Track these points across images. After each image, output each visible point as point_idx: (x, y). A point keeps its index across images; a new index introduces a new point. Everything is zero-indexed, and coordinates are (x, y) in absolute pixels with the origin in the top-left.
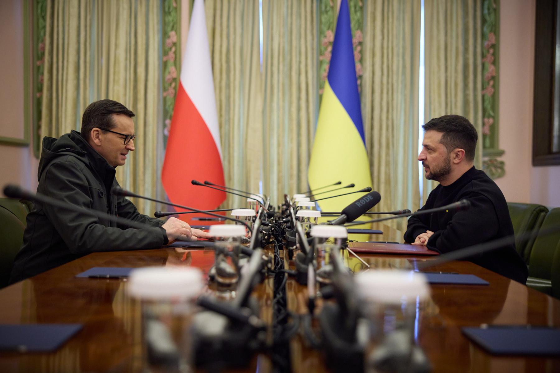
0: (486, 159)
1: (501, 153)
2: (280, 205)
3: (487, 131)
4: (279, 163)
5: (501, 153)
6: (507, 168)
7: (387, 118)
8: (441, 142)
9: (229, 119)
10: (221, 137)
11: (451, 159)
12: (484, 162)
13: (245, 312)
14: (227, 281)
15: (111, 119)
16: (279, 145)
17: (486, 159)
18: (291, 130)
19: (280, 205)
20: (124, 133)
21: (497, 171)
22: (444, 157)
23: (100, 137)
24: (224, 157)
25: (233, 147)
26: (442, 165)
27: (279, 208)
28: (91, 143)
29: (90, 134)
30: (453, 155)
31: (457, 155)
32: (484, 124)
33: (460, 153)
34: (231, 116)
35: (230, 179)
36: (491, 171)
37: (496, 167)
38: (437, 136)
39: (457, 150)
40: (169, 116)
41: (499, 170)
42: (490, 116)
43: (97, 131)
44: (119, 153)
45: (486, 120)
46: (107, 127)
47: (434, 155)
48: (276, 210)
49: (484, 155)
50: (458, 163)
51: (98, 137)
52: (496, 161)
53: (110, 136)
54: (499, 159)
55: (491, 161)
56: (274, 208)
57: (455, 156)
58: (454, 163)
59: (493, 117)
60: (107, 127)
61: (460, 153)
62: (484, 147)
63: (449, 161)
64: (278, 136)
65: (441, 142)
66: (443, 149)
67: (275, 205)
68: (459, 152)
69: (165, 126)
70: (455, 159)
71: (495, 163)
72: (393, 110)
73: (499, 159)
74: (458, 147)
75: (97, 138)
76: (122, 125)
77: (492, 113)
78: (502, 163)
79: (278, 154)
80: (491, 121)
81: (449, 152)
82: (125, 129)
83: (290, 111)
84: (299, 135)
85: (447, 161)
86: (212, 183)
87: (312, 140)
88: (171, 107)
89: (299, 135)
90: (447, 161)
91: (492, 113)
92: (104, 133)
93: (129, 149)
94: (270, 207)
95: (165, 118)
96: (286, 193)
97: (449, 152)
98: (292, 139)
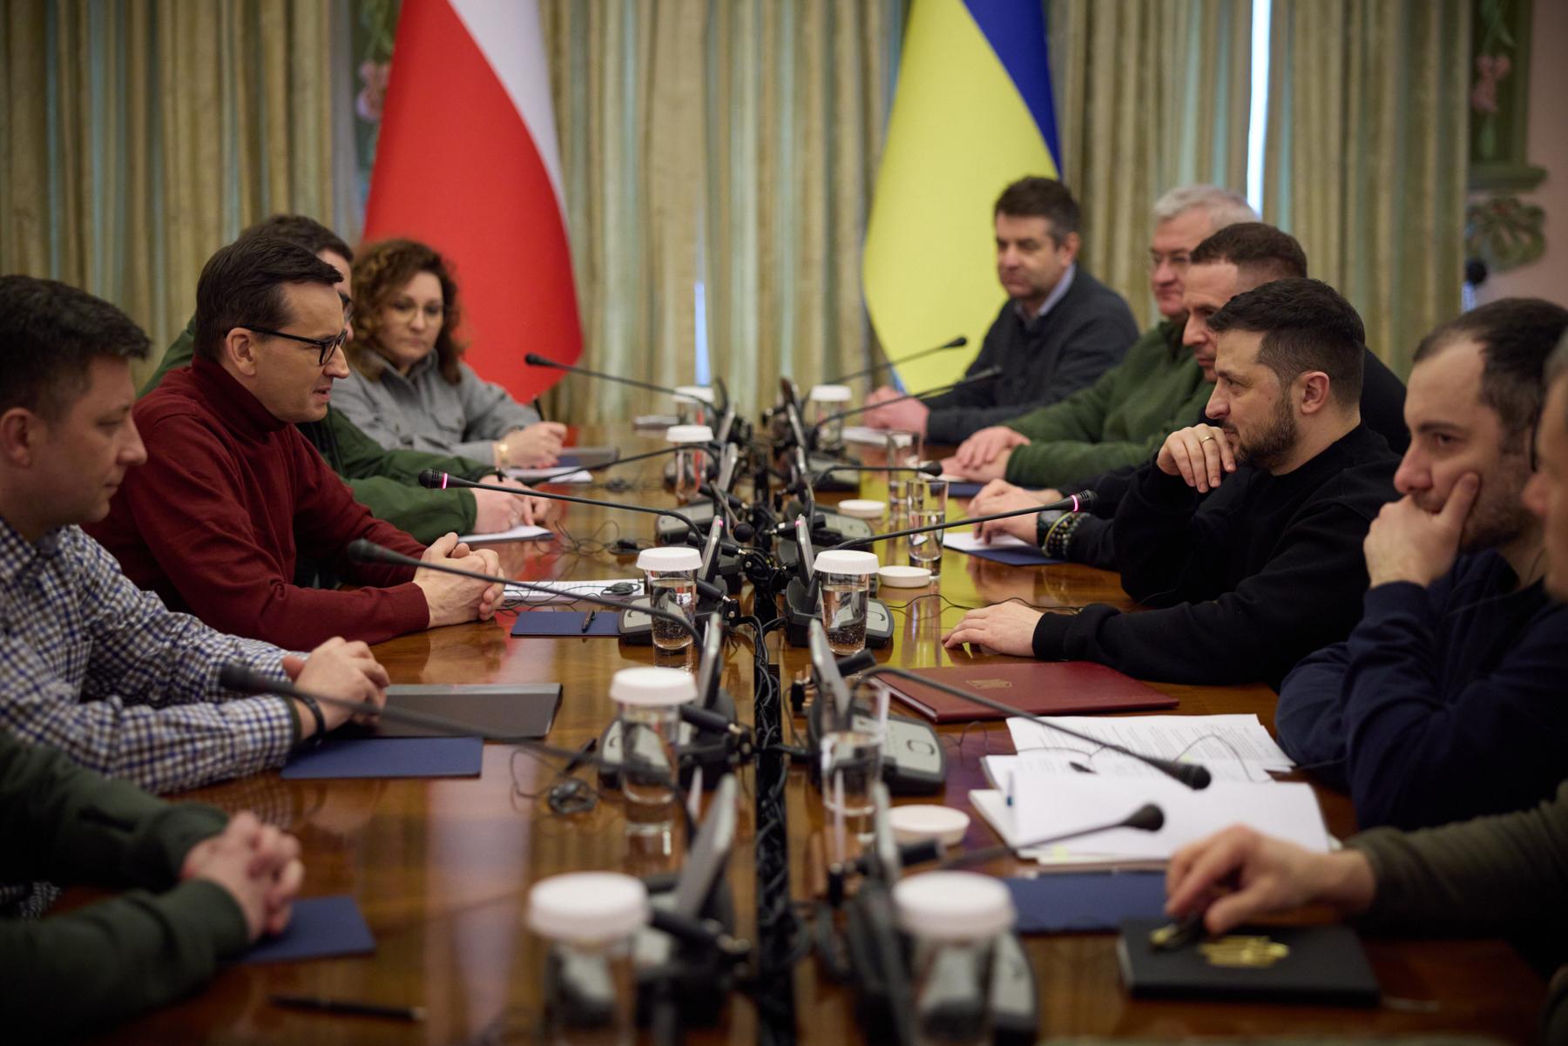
0: (1482, 198)
1: (1535, 178)
2: (769, 412)
3: (1487, 101)
4: (763, 221)
5: (1535, 178)
6: (1550, 230)
7: (1142, 59)
9: (587, 63)
10: (559, 128)
11: (1295, 402)
12: (1473, 212)
13: (711, 927)
14: (650, 799)
15: (279, 300)
16: (761, 157)
17: (1482, 198)
18: (801, 101)
19: (769, 412)
20: (317, 334)
21: (1515, 238)
22: (1274, 401)
23: (252, 351)
24: (570, 196)
25: (602, 164)
26: (1269, 420)
27: (764, 420)
28: (227, 366)
29: (224, 345)
30: (1297, 393)
31: (1310, 392)
32: (1476, 76)
34: (594, 56)
35: (593, 274)
36: (1497, 240)
37: (1513, 226)
40: (371, 50)
41: (1526, 238)
42: (1498, 48)
43: (243, 336)
44: (308, 390)
45: (1485, 61)
46: (269, 322)
47: (1248, 397)
48: (757, 429)
49: (1474, 185)
50: (1316, 413)
51: (245, 353)
52: (1517, 204)
53: (278, 345)
54: (1527, 199)
55: (1497, 205)
56: (749, 428)
57: (1303, 393)
58: (1304, 414)
59: (1512, 53)
60: (269, 322)
62: (1475, 156)
63: (1289, 408)
64: (760, 125)
66: (1267, 376)
67: (751, 418)
69: (358, 85)
70: (1305, 401)
71: (1513, 212)
72: (1160, 30)
73: (1527, 199)
74: (1309, 368)
75: (243, 356)
76: (310, 313)
77: (1507, 39)
78: (1536, 213)
79: (760, 187)
80: (1503, 63)
81: (1287, 385)
82: (319, 324)
83: (799, 31)
84: (832, 118)
85: (1285, 408)
86: (548, 359)
87: (876, 137)
88: (380, 18)
89: (832, 118)
90: (1285, 408)
91: (1507, 39)
92: (262, 340)
93: (332, 376)
94: (738, 421)
95: (357, 60)
96: (787, 372)
97: (1287, 385)
98: (807, 136)
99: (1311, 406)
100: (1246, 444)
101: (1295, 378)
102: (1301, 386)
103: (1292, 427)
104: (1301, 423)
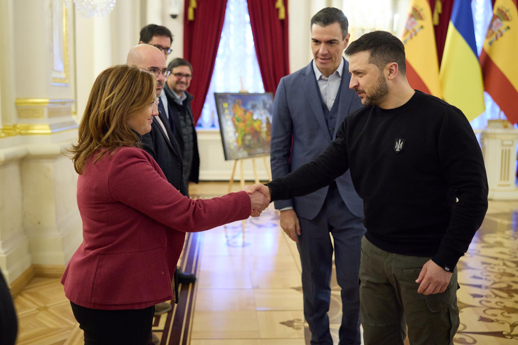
8: (370, 62)
26: (377, 85)
30: (386, 72)
31: (391, 71)
33: (394, 68)
39: (389, 65)
47: (365, 77)
57: (388, 72)
61: (394, 68)
63: (384, 78)
65: (370, 62)
66: (373, 68)
68: (391, 66)
74: (389, 62)
81: (382, 70)
90: (383, 79)
97: (382, 70)
99: (392, 76)
103: (386, 85)
104: (390, 83)
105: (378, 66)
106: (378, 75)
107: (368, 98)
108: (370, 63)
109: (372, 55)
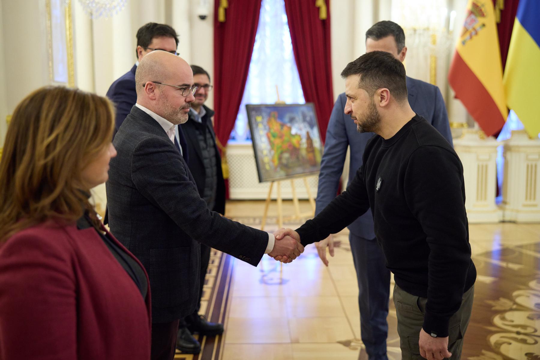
8: (360, 87)
26: (367, 112)
30: (377, 98)
31: (382, 98)
38: (355, 79)
39: (380, 91)
61: (385, 94)
63: (374, 106)
65: (360, 87)
66: (363, 94)
68: (382, 92)
70: (381, 101)
74: (380, 87)
81: (372, 96)
85: (373, 106)
90: (373, 106)
97: (372, 96)
99: (384, 103)
100: (360, 123)
101: (375, 92)
102: (379, 95)
103: (377, 113)
104: (381, 111)
105: (367, 91)
106: (368, 102)
107: (360, 125)
108: (360, 88)
109: (362, 79)
